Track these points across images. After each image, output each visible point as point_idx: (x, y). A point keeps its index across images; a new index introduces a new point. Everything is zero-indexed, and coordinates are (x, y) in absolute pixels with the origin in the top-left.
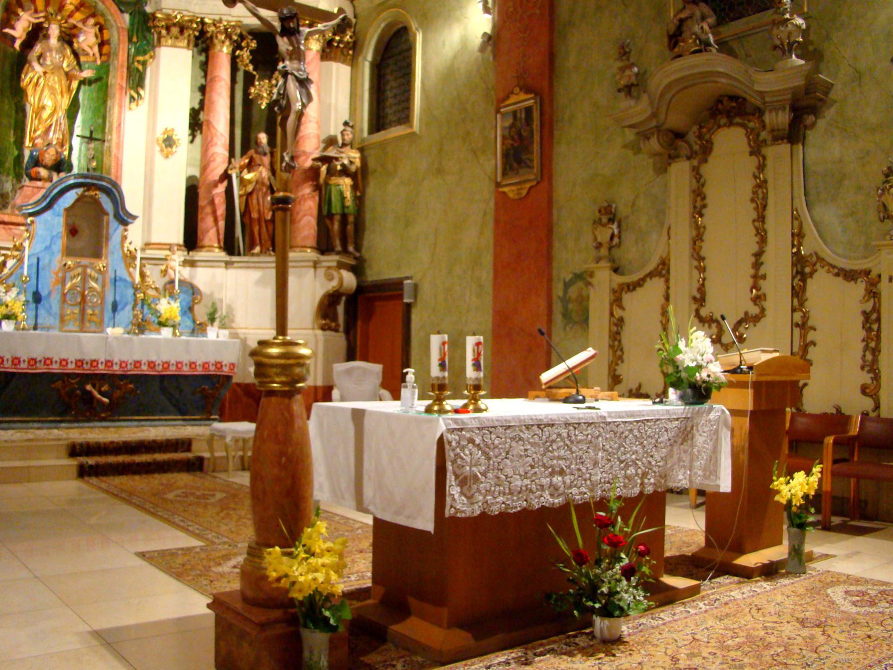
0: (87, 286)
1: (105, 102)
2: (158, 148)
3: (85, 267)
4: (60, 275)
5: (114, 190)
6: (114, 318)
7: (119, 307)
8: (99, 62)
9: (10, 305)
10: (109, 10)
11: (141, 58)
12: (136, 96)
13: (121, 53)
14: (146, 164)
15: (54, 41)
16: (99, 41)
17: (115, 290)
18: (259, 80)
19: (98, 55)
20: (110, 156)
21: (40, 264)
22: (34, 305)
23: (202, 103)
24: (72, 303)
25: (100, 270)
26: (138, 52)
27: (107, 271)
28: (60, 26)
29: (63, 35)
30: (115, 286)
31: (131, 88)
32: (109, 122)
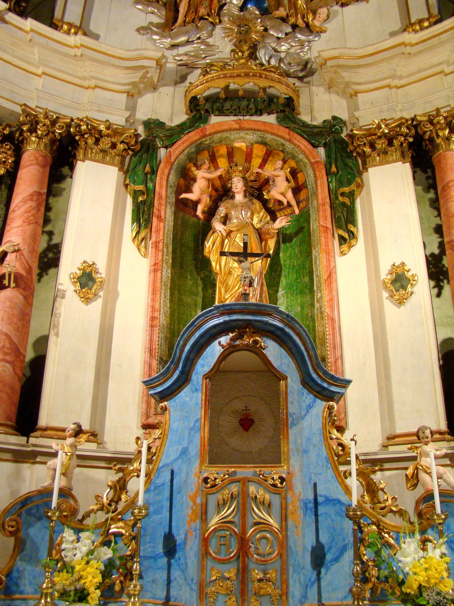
0: (250, 521)
1: (309, 254)
2: (385, 294)
3: (245, 482)
4: (198, 501)
5: (287, 330)
6: (319, 579)
7: (329, 557)
8: (297, 212)
9: (78, 568)
10: (298, 146)
11: (346, 190)
12: (346, 236)
13: (319, 191)
14: (373, 320)
15: (239, 198)
17: (317, 521)
19: (293, 203)
21: (175, 481)
22: (165, 560)
23: (441, 245)
24: (222, 557)
25: (274, 485)
26: (340, 184)
27: (290, 488)
28: (244, 178)
29: (251, 190)
30: (316, 515)
31: (339, 227)
32: (317, 276)
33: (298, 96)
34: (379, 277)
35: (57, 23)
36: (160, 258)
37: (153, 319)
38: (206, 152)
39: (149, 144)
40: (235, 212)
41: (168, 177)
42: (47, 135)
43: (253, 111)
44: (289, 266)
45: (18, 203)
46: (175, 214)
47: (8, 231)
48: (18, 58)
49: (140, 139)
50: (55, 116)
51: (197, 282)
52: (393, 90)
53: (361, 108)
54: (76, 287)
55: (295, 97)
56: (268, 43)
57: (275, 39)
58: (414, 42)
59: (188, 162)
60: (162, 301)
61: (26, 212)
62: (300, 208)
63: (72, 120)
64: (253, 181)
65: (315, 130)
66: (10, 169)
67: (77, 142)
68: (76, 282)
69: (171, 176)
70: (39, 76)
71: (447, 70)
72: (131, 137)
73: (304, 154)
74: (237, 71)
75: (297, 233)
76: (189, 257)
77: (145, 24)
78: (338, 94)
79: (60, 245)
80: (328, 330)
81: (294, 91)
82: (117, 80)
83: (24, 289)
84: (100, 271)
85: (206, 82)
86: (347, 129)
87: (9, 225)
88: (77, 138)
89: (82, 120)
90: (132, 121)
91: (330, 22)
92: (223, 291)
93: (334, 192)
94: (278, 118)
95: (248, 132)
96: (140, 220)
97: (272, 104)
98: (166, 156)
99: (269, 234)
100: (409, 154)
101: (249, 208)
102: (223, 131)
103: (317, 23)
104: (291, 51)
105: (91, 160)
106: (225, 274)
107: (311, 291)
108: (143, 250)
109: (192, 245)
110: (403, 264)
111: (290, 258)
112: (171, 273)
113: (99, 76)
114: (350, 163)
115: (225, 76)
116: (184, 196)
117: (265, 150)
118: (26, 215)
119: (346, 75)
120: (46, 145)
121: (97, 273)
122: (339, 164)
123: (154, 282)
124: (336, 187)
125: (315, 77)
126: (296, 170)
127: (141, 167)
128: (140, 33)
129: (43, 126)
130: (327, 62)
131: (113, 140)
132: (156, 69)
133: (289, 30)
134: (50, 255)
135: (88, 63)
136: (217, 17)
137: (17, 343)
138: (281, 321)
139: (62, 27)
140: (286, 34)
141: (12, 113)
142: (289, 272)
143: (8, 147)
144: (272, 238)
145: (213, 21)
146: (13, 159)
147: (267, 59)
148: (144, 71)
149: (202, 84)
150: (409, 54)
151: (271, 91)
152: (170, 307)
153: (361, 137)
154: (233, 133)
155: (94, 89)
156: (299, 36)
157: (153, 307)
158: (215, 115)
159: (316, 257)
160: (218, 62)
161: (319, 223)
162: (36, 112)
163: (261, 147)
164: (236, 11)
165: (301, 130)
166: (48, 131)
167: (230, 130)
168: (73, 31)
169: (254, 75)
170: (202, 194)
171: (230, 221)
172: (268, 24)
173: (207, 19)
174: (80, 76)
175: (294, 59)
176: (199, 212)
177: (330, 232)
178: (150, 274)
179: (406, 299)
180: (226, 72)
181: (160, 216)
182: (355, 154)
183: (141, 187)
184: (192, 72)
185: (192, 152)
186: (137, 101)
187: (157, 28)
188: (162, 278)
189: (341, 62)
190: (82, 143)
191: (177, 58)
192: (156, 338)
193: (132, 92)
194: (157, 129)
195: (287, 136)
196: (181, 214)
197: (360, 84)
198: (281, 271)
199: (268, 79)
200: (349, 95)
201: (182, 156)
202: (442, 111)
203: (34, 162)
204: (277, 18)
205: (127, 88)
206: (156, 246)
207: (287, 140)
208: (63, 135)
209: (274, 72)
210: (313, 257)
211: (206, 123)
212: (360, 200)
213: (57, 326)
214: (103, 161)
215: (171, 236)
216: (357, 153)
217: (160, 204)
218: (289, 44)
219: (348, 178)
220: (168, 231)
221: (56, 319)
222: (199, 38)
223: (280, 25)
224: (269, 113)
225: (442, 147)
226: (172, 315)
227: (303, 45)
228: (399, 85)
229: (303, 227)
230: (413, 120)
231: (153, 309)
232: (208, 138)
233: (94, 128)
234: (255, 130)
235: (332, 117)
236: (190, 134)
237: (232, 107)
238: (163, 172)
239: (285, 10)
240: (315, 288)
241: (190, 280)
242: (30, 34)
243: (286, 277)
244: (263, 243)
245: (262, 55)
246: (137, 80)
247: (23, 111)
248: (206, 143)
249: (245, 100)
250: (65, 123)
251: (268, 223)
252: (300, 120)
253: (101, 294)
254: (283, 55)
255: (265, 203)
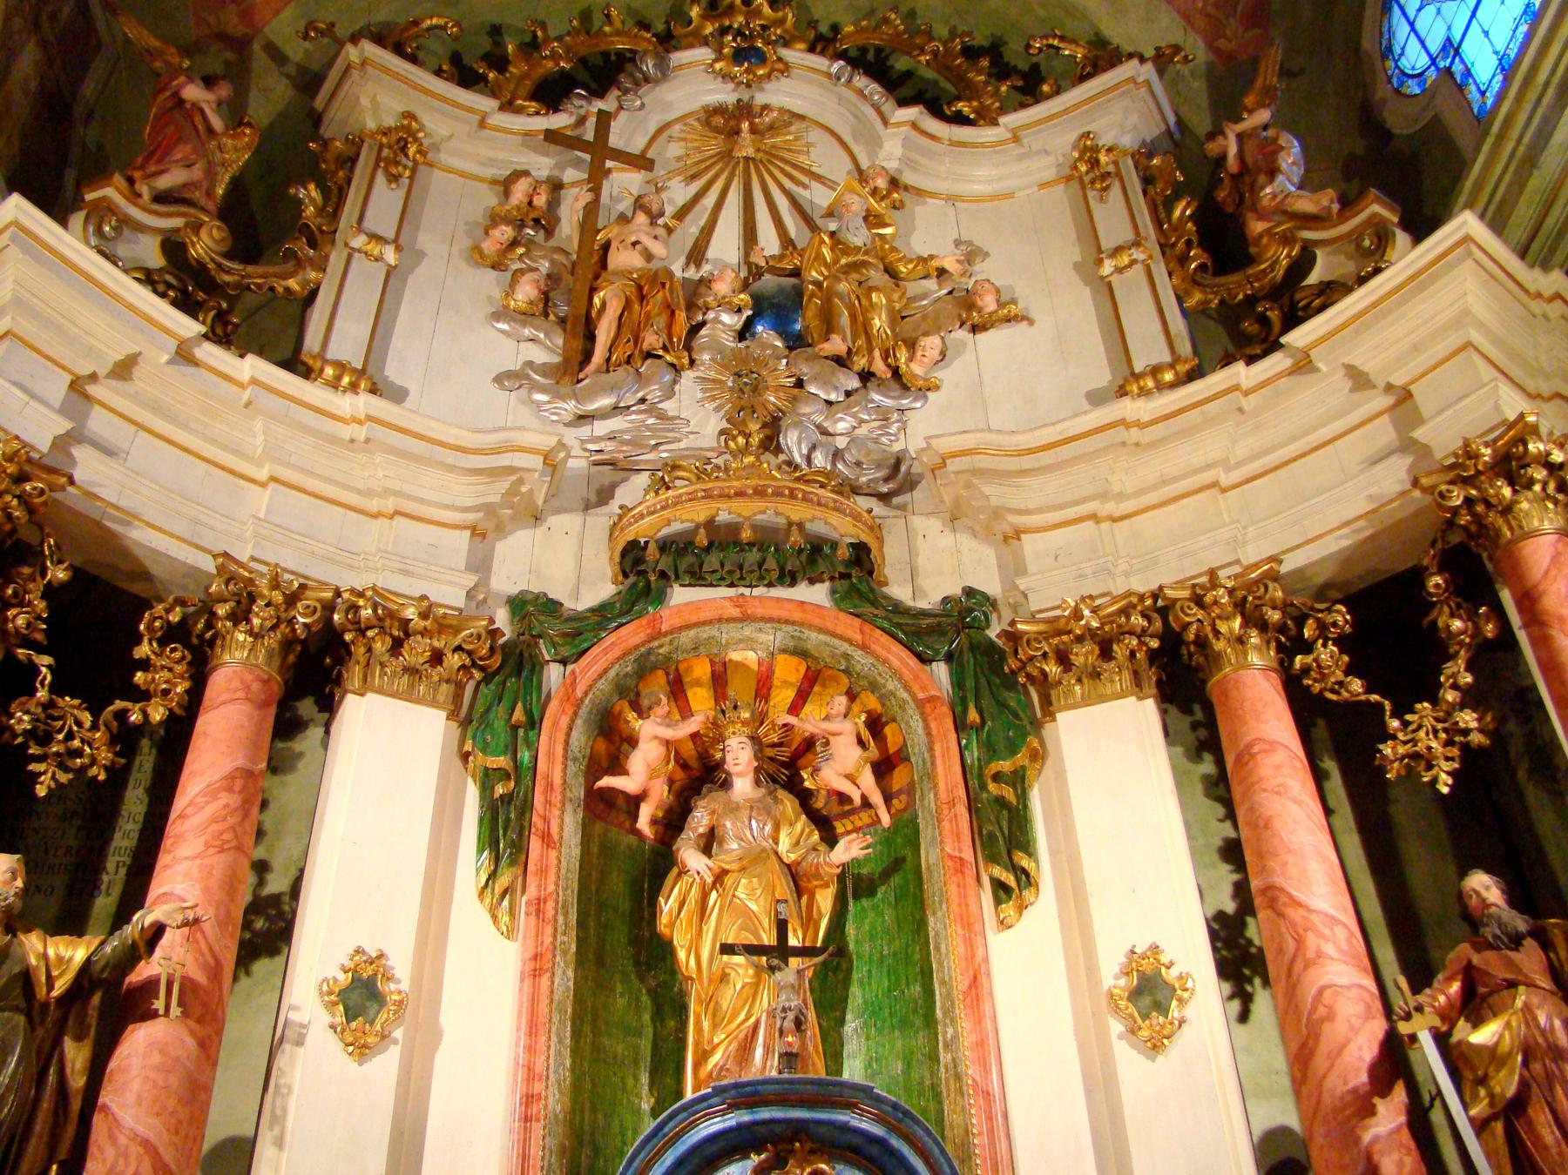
1: (920, 926)
2: (1116, 1027)
5: (896, 1143)
8: (886, 819)
10: (885, 661)
11: (1005, 765)
12: (1010, 880)
13: (940, 769)
14: (1089, 1091)
15: (743, 786)
16: (874, 752)
18: (1394, 715)
19: (877, 798)
20: (961, 1092)
23: (1241, 891)
26: (991, 750)
28: (755, 739)
29: (771, 768)
31: (992, 858)
32: (943, 983)
33: (881, 540)
34: (1098, 983)
35: (311, 362)
36: (548, 940)
37: (529, 1099)
38: (660, 673)
39: (521, 654)
40: (733, 823)
41: (568, 735)
42: (274, 628)
43: (775, 575)
44: (871, 955)
45: (196, 795)
46: (586, 827)
47: (166, 867)
48: (215, 442)
49: (501, 641)
50: (296, 584)
51: (638, 1000)
52: (1105, 526)
53: (1030, 569)
54: (333, 1015)
55: (873, 544)
56: (804, 415)
57: (822, 406)
58: (1145, 418)
59: (616, 698)
60: (552, 1053)
61: (214, 820)
62: (893, 811)
63: (338, 594)
64: (774, 745)
65: (925, 622)
66: (178, 711)
67: (346, 646)
68: (335, 1004)
69: (575, 734)
70: (263, 485)
71: (1226, 479)
72: (479, 637)
73: (900, 679)
74: (735, 483)
75: (886, 875)
76: (619, 935)
77: (515, 366)
78: (975, 534)
79: (286, 899)
80: (977, 1122)
81: (871, 528)
82: (448, 500)
83: (199, 1021)
84: (398, 973)
85: (663, 508)
86: (999, 618)
87: (169, 852)
88: (348, 637)
89: (361, 595)
90: (481, 597)
91: (947, 366)
92: (706, 1025)
93: (975, 772)
94: (833, 592)
95: (762, 625)
96: (498, 842)
97: (820, 561)
98: (564, 684)
99: (818, 876)
100: (1151, 676)
101: (769, 813)
102: (704, 623)
103: (917, 369)
104: (858, 432)
105: (380, 691)
106: (710, 981)
107: (930, 1021)
108: (505, 919)
109: (625, 905)
110: (1155, 949)
111: (872, 937)
112: (575, 978)
113: (408, 489)
114: (1012, 699)
115: (708, 495)
116: (606, 781)
117: (803, 669)
118: (214, 827)
119: (994, 492)
120: (270, 655)
121: (388, 979)
122: (985, 703)
123: (534, 1001)
124: (979, 759)
125: (918, 494)
126: (880, 715)
127: (500, 711)
128: (503, 388)
129: (267, 605)
130: (948, 461)
131: (436, 644)
132: (543, 474)
133: (854, 383)
134: (260, 924)
135: (378, 458)
136: (686, 354)
137: (173, 1167)
138: (879, 1119)
139: (322, 370)
140: (848, 394)
141: (193, 572)
142: (870, 971)
143: (178, 655)
144: (826, 885)
145: (675, 361)
146: (187, 684)
147: (805, 451)
148: (513, 478)
149: (653, 513)
150: (1137, 444)
151: (818, 527)
152: (573, 1063)
153: (1035, 639)
154: (725, 627)
155: (391, 517)
156: (877, 397)
157: (530, 1069)
158: (681, 585)
159: (937, 934)
160: (687, 457)
161: (942, 850)
162: (251, 572)
163: (794, 660)
164: (729, 341)
165: (890, 620)
166: (278, 618)
167: (720, 620)
168: (346, 380)
169: (778, 493)
170: (651, 778)
171: (720, 844)
172: (805, 370)
173: (659, 357)
174: (360, 486)
175: (868, 453)
176: (643, 823)
177: (970, 873)
178: (522, 981)
179: (1168, 1038)
180: (710, 485)
181: (549, 834)
182: (1022, 680)
183: (502, 761)
184: (624, 480)
185: (626, 675)
186: (493, 549)
187: (544, 375)
188: (552, 992)
189: (982, 462)
190: (359, 651)
191: (592, 447)
192: (536, 1151)
193: (482, 526)
194: (542, 618)
195: (858, 637)
196: (599, 827)
197: (1027, 512)
198: (850, 970)
199: (811, 501)
200: (1000, 537)
201: (604, 685)
202: (1222, 574)
203: (240, 694)
204: (826, 358)
205: (471, 517)
206: (538, 911)
207: (857, 646)
208: (314, 629)
209: (823, 486)
210: (932, 934)
211: (661, 603)
212: (1040, 790)
213: (279, 1120)
214: (408, 696)
215: (575, 885)
216: (1028, 676)
217: (548, 802)
218: (854, 416)
219: (1008, 738)
220: (568, 870)
221: (279, 1102)
222: (643, 400)
223: (833, 373)
224: (812, 581)
225: (1229, 660)
226: (577, 1087)
227: (886, 419)
228: (1116, 514)
229: (904, 860)
230: (1155, 596)
231: (531, 1075)
232: (667, 639)
233: (392, 615)
234: (779, 621)
235: (964, 589)
236: (623, 630)
237: (722, 565)
238: (555, 724)
239: (844, 339)
240: (939, 1013)
241: (622, 995)
242: (248, 391)
243: (861, 983)
244: (805, 899)
245: (793, 441)
246: (497, 499)
247: (221, 569)
248: (661, 651)
249: (755, 550)
250: (319, 600)
251: (815, 849)
252: (887, 598)
253: (398, 1034)
254: (841, 443)
255: (804, 798)
